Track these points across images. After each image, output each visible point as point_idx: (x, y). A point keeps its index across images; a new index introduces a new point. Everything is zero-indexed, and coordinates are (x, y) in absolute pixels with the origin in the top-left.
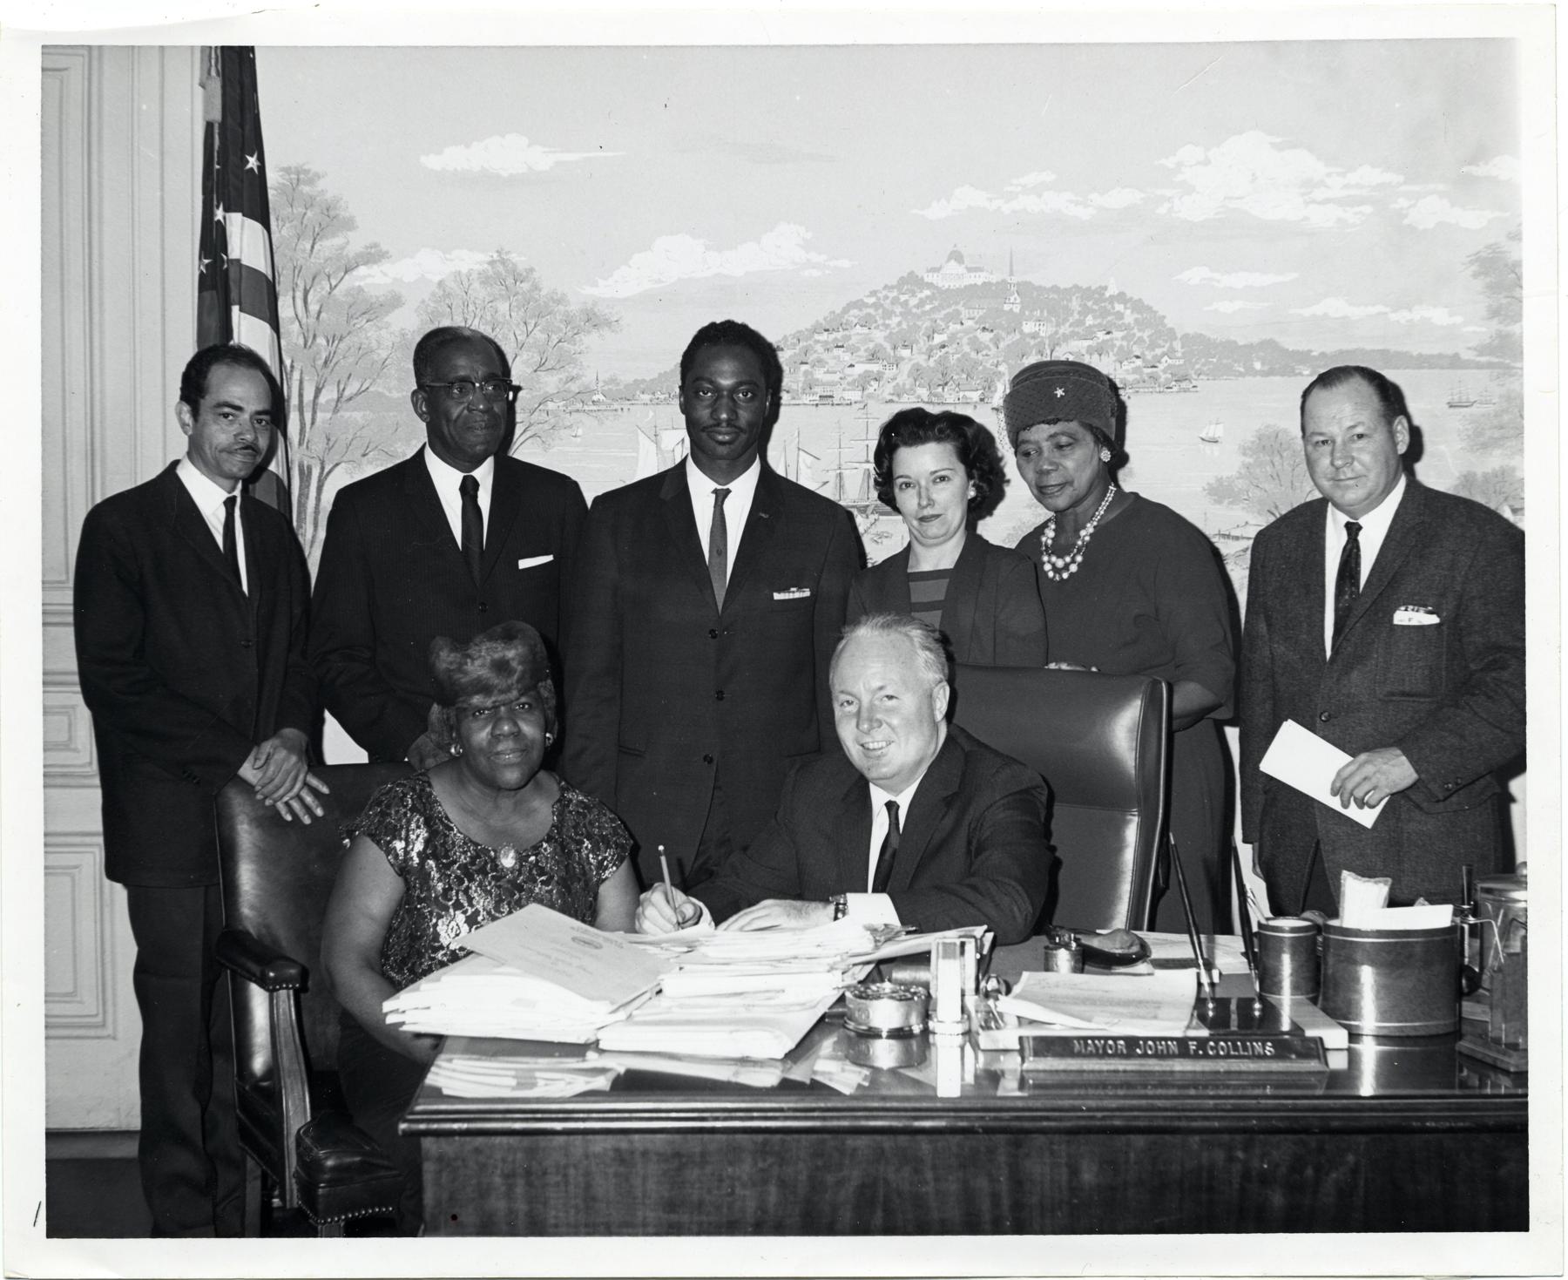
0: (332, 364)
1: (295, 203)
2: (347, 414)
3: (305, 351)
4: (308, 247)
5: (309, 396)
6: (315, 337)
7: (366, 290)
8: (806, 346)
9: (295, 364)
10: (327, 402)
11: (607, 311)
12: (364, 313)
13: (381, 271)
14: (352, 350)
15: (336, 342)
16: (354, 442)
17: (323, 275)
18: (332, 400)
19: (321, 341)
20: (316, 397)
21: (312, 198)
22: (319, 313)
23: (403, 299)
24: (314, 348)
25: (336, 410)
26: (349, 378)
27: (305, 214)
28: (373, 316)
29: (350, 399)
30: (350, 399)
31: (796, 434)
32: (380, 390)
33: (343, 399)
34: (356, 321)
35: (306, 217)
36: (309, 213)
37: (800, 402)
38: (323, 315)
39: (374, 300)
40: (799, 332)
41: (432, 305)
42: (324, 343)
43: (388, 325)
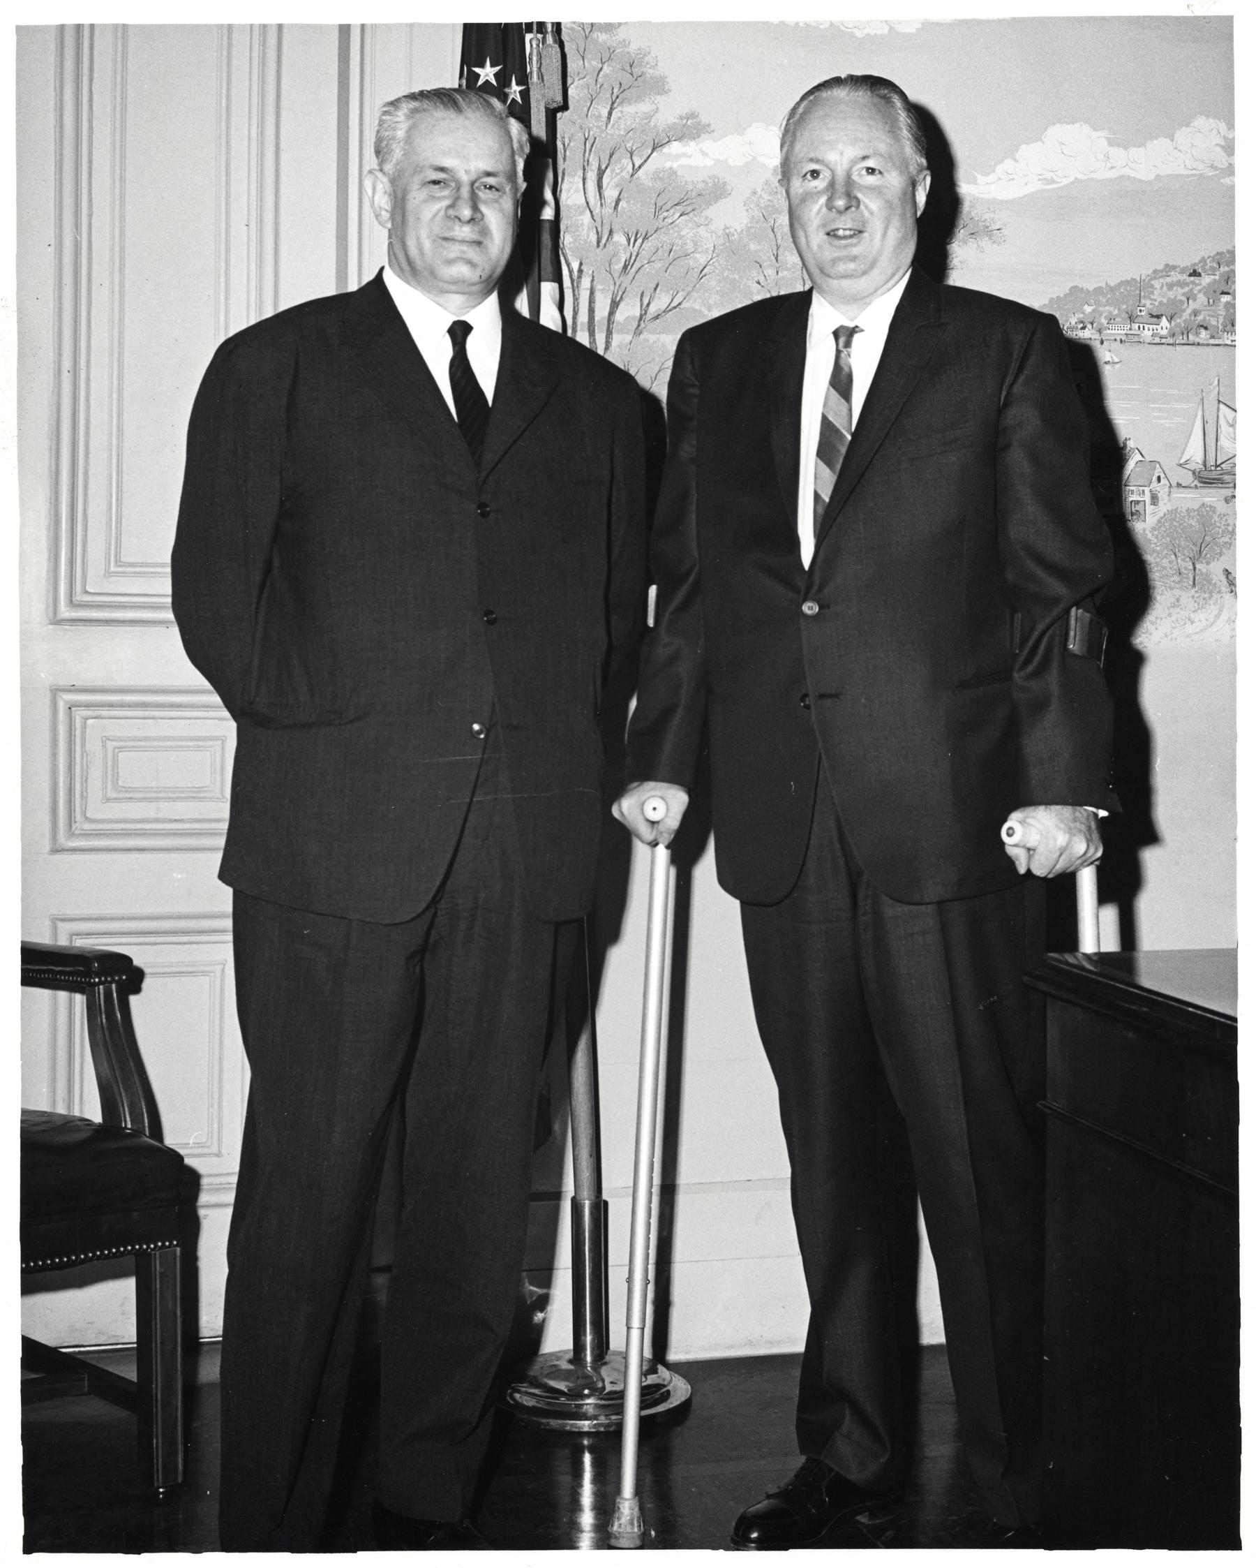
0: (634, 270)
1: (588, 56)
2: (652, 338)
3: (598, 250)
4: (605, 113)
5: (602, 311)
6: (611, 232)
7: (679, 173)
8: (1227, 272)
9: (584, 268)
10: (627, 319)
11: (987, 216)
12: (676, 205)
13: (701, 150)
14: (660, 250)
15: (640, 241)
16: (661, 373)
17: (622, 150)
18: (634, 318)
19: (619, 238)
20: (612, 313)
21: (611, 51)
22: (618, 201)
23: (729, 188)
24: (610, 247)
25: (638, 332)
26: (655, 289)
27: (601, 69)
28: (689, 209)
29: (657, 317)
30: (657, 317)
31: (1216, 382)
32: (697, 307)
33: (649, 316)
34: (666, 214)
35: (602, 73)
36: (606, 69)
37: (1220, 342)
38: (621, 203)
39: (690, 187)
40: (1218, 253)
41: (766, 197)
42: (623, 241)
43: (709, 221)
